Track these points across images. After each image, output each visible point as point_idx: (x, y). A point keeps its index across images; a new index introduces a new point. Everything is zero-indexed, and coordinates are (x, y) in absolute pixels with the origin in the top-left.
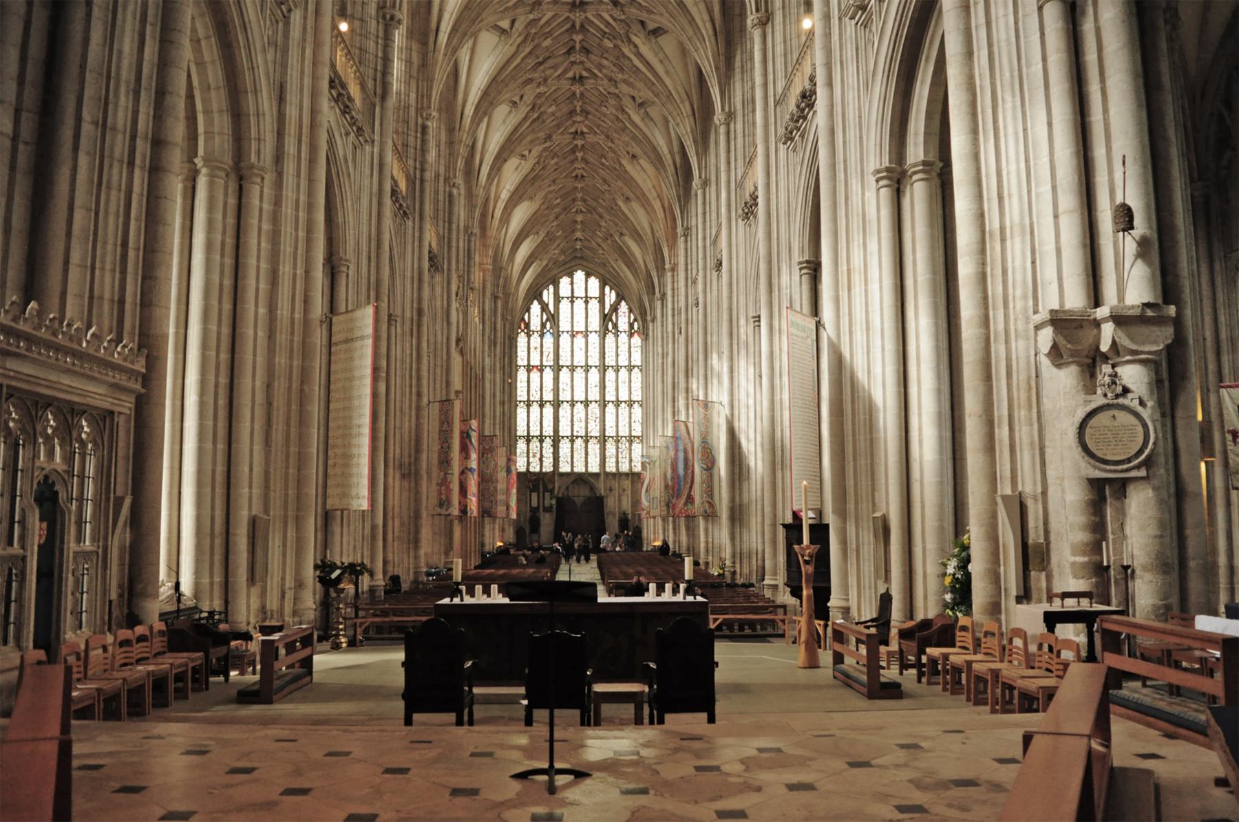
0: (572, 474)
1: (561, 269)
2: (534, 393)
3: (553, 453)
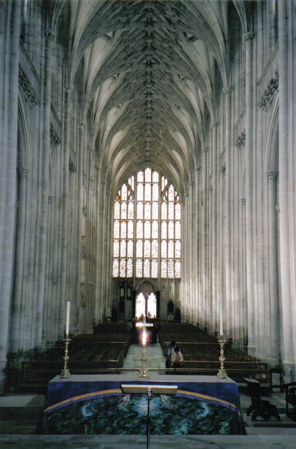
0: (143, 278)
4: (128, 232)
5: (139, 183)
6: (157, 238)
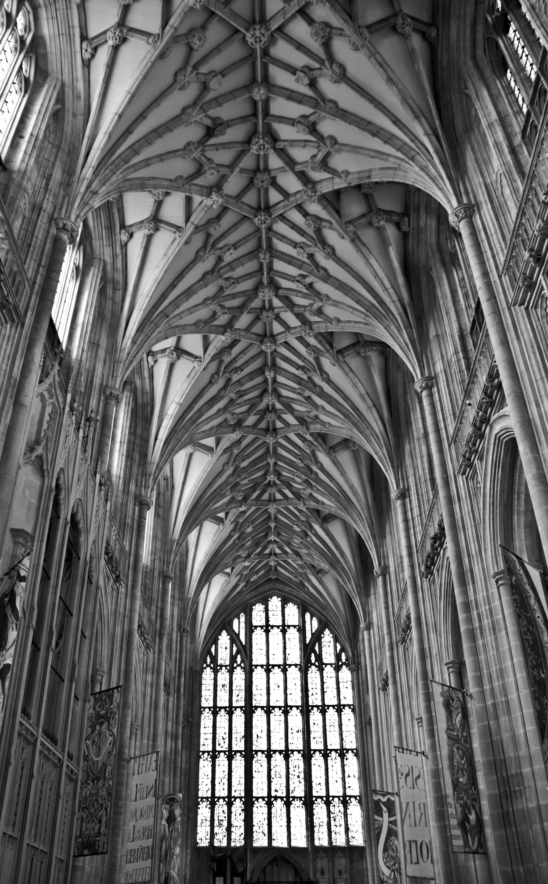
1: (253, 593)
2: (221, 741)
4: (234, 736)
5: (256, 627)
6: (301, 747)
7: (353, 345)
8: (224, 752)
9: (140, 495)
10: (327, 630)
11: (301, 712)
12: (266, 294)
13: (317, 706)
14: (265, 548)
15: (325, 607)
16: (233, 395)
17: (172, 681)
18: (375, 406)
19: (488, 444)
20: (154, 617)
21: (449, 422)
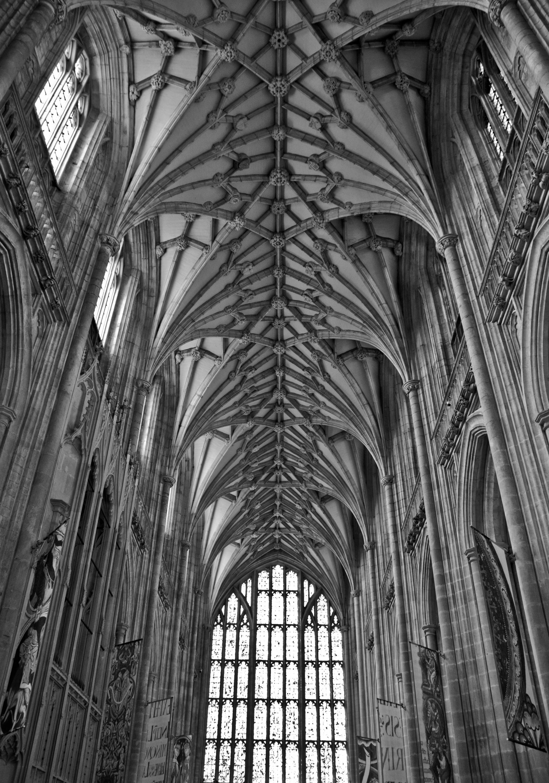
1: (259, 562)
2: (228, 690)
3: (246, 760)
4: (239, 686)
5: (261, 591)
6: (296, 697)
7: (352, 351)
8: (230, 699)
9: (165, 474)
10: (322, 595)
11: (298, 666)
12: (278, 305)
13: (312, 662)
14: (271, 523)
15: (321, 575)
16: (247, 391)
17: (187, 636)
18: (368, 404)
19: (464, 439)
20: (173, 580)
21: (432, 420)
